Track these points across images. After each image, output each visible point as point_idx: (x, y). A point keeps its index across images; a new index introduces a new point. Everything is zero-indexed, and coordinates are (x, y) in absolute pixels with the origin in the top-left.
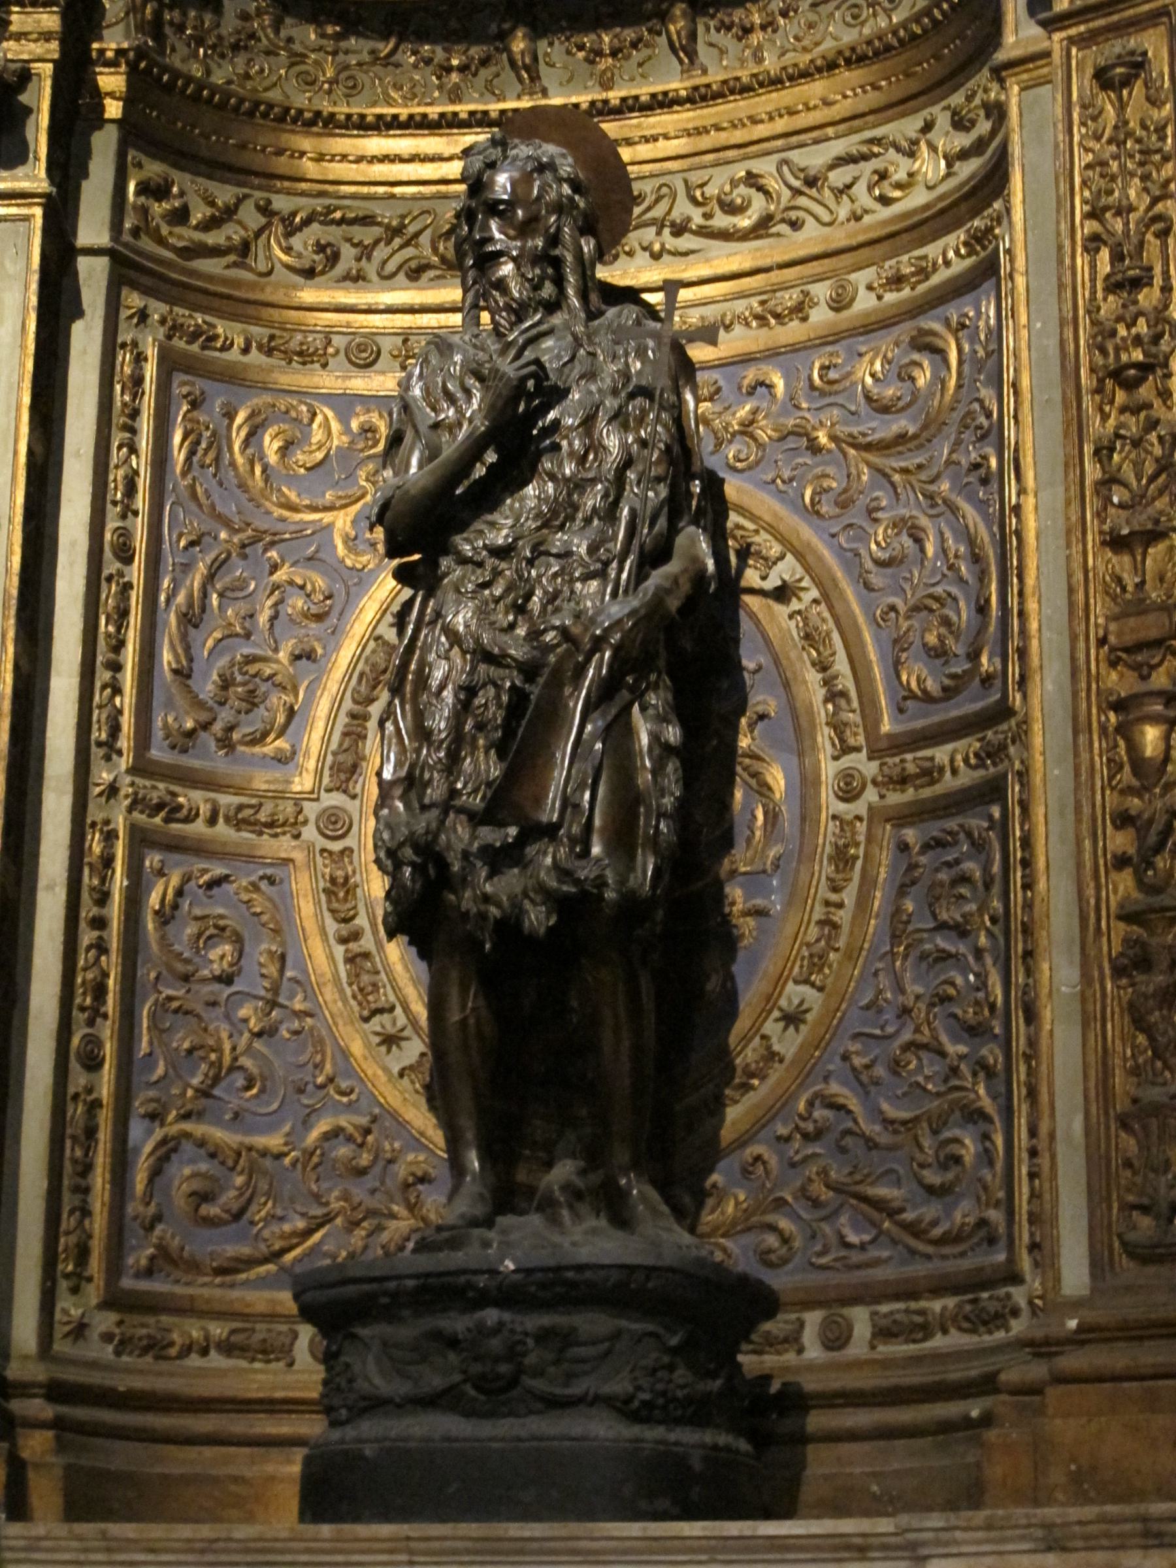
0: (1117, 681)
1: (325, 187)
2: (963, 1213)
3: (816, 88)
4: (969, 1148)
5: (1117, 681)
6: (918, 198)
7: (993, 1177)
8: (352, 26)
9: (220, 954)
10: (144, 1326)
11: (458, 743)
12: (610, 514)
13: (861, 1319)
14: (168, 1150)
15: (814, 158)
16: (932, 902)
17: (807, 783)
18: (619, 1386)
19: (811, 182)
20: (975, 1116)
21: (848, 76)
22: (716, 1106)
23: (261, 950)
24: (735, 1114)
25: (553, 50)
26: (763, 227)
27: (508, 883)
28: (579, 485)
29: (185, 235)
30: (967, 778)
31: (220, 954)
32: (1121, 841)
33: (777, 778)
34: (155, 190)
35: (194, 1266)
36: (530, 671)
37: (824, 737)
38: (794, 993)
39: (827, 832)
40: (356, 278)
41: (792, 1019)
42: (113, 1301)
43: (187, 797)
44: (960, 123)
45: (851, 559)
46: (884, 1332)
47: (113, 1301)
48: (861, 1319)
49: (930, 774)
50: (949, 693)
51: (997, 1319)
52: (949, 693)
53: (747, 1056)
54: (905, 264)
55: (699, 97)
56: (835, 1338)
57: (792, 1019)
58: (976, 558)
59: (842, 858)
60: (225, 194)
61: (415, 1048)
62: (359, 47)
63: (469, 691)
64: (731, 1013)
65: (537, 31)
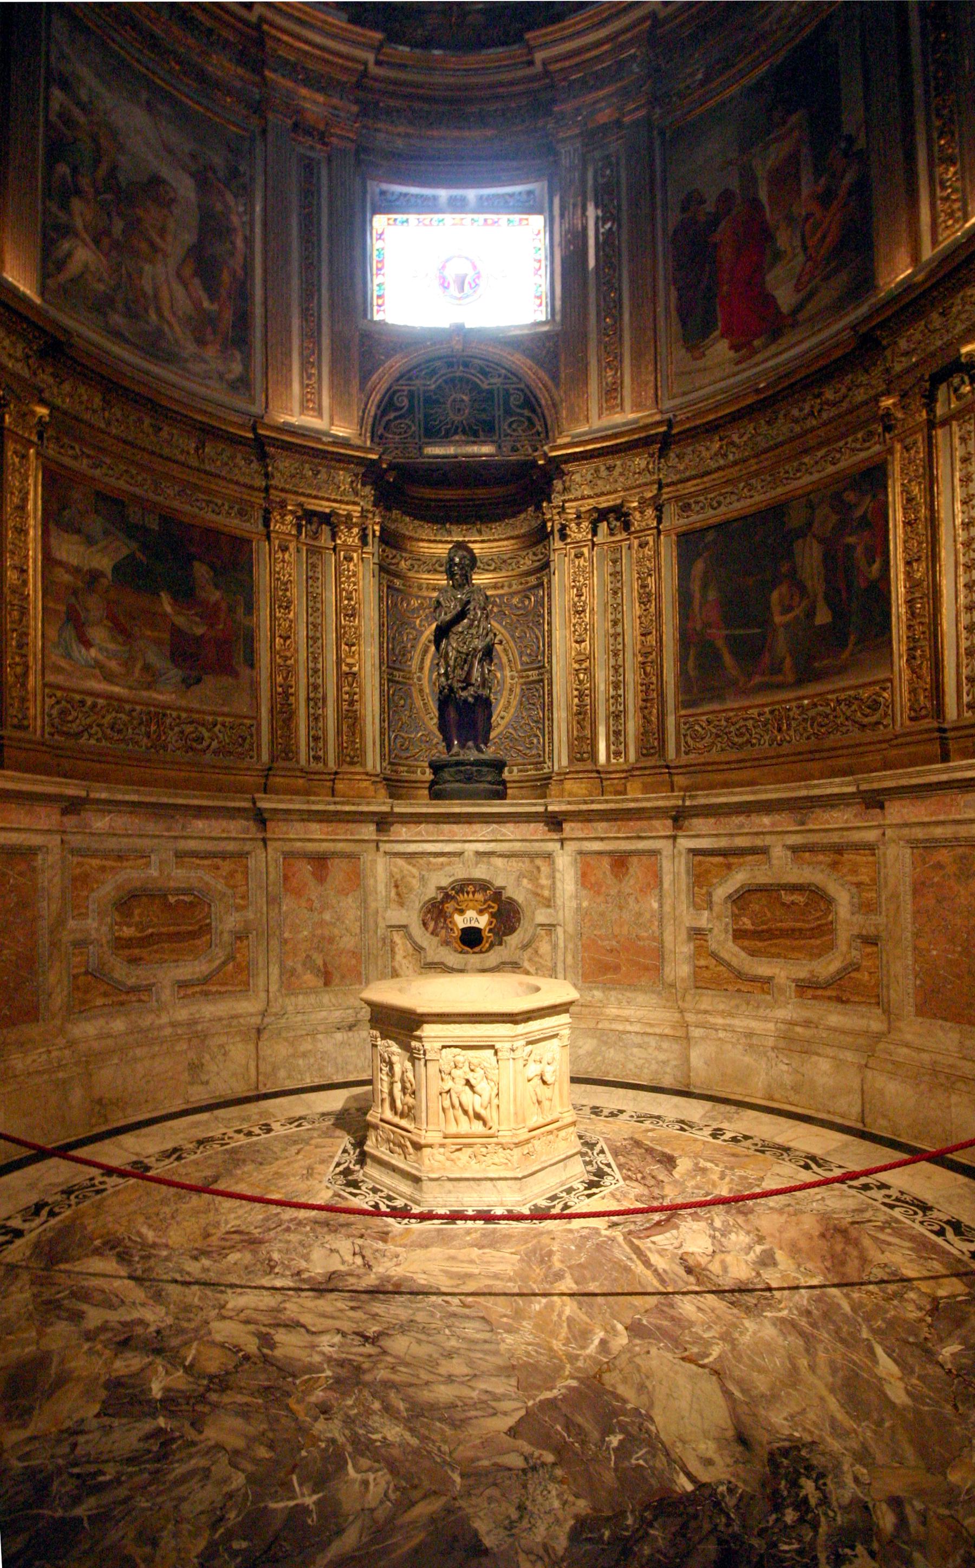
0: (576, 666)
1: (411, 552)
2: (534, 752)
3: (505, 543)
4: (535, 741)
5: (576, 666)
6: (524, 568)
7: (540, 747)
8: (416, 518)
9: (402, 702)
10: (395, 768)
11: (455, 667)
12: (478, 626)
13: (515, 769)
14: (396, 737)
15: (505, 557)
16: (528, 699)
17: (504, 677)
18: (489, 778)
19: (504, 561)
20: (536, 736)
21: (513, 542)
22: (488, 732)
23: (409, 701)
24: (493, 735)
25: (454, 528)
26: (494, 570)
27: (464, 694)
28: (473, 621)
29: (388, 561)
30: (535, 678)
31: (402, 702)
32: (576, 693)
33: (499, 675)
34: (384, 551)
35: (401, 758)
36: (467, 655)
37: (508, 669)
38: (502, 714)
39: (508, 686)
40: (417, 572)
41: (502, 718)
42: (390, 763)
43: (396, 673)
44: (535, 554)
45: (513, 636)
46: (520, 771)
47: (390, 763)
48: (515, 769)
49: (528, 677)
50: (532, 663)
51: (542, 769)
52: (532, 663)
53: (494, 724)
54: (523, 580)
55: (483, 541)
56: (511, 772)
57: (502, 718)
58: (537, 638)
59: (511, 690)
60: (394, 552)
61: (435, 720)
62: (417, 523)
63: (456, 659)
64: (490, 716)
65: (451, 524)
